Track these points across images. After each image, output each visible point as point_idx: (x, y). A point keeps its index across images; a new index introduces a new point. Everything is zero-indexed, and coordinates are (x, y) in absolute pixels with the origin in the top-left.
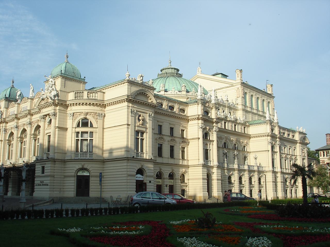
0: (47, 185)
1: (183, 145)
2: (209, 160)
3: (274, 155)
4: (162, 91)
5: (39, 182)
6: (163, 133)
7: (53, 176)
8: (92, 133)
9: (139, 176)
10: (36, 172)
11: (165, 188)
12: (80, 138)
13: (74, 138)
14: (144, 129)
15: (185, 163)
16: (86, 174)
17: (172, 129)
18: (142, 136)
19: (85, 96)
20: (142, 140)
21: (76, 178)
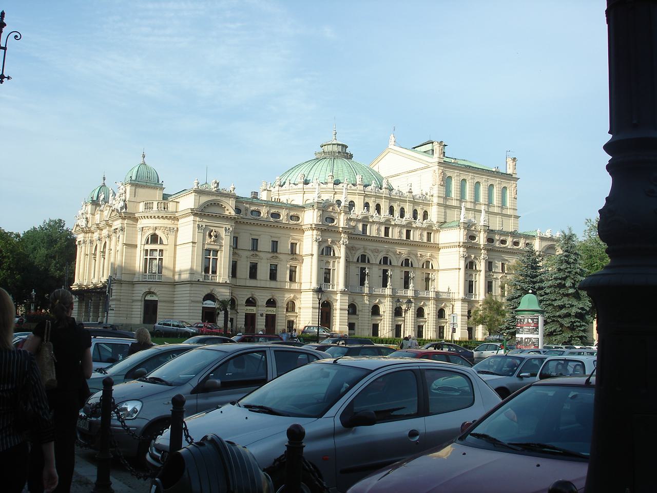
1: (293, 263)
2: (331, 283)
3: (474, 275)
4: (300, 183)
7: (119, 300)
9: (209, 302)
11: (260, 317)
12: (148, 257)
13: (143, 257)
14: (217, 248)
15: (295, 286)
16: (154, 298)
21: (143, 303)
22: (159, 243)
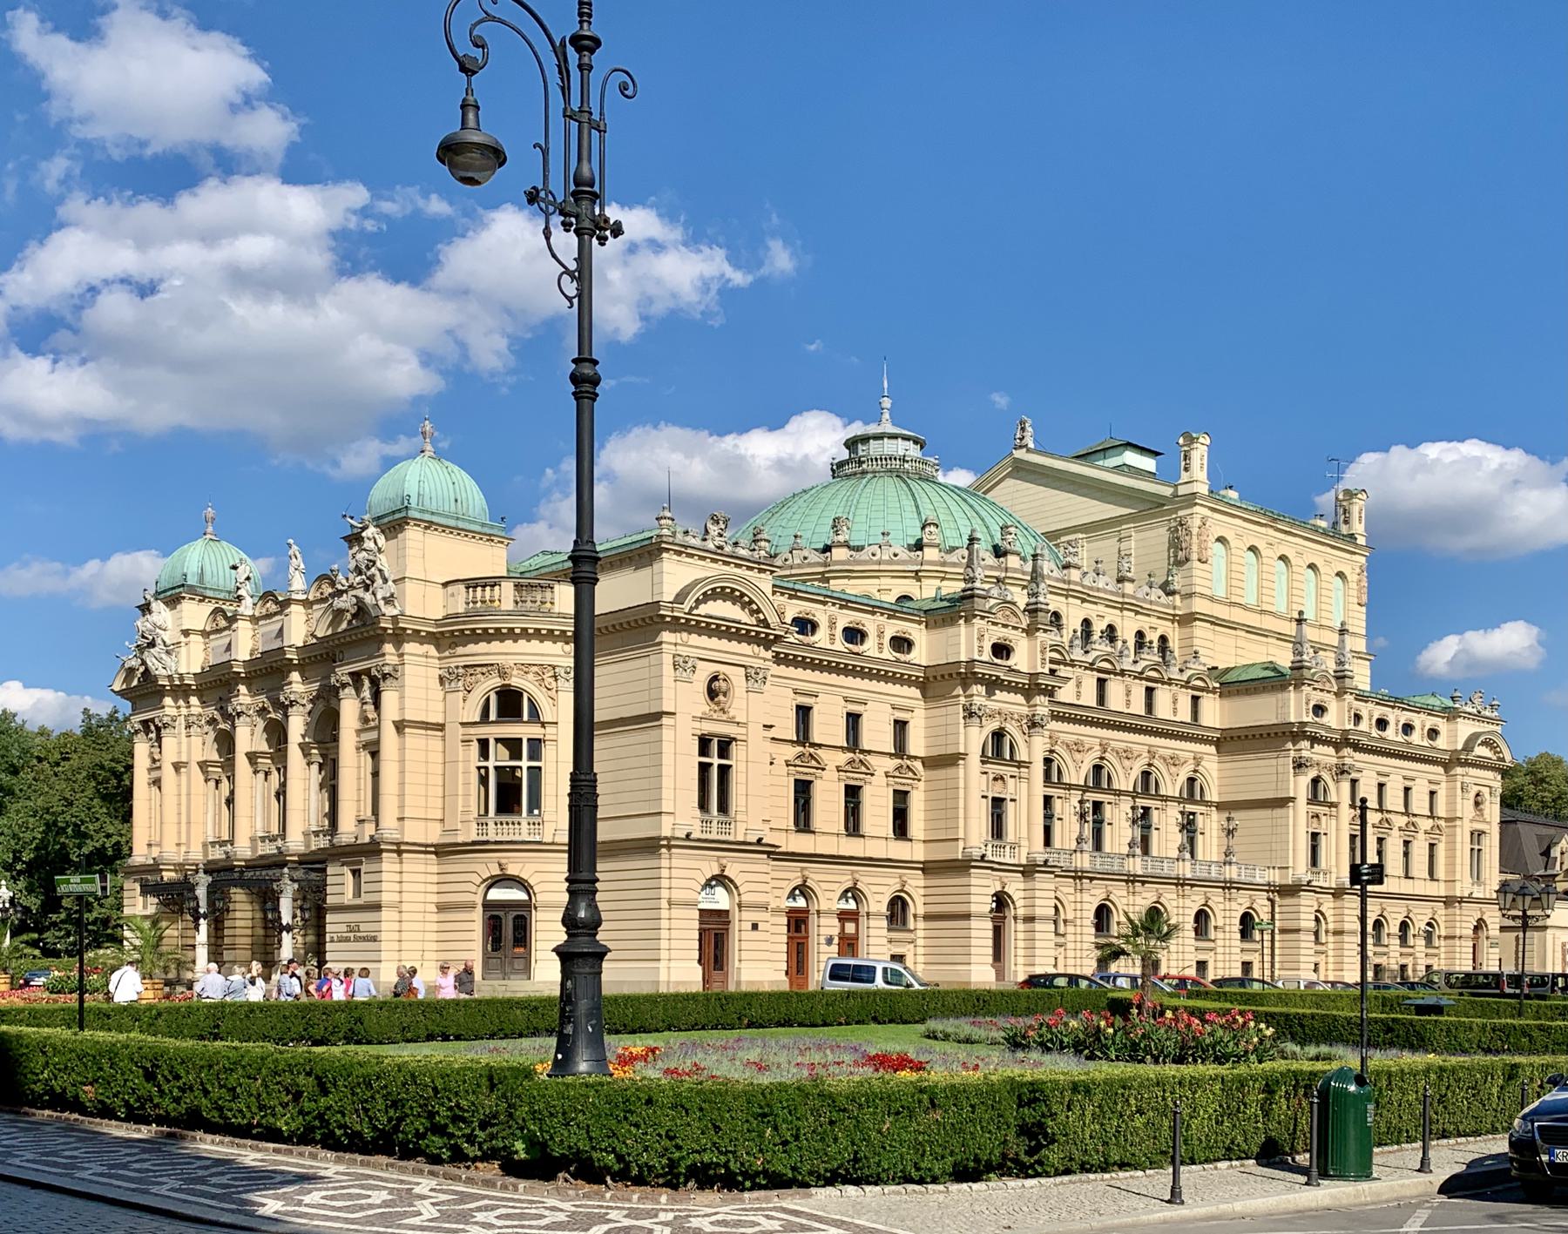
0: (374, 939)
5: (344, 928)
6: (816, 737)
8: (536, 745)
10: (329, 889)
11: (824, 948)
16: (518, 895)
17: (853, 720)
18: (724, 751)
19: (508, 604)
20: (724, 771)
21: (478, 915)
22: (525, 718)
